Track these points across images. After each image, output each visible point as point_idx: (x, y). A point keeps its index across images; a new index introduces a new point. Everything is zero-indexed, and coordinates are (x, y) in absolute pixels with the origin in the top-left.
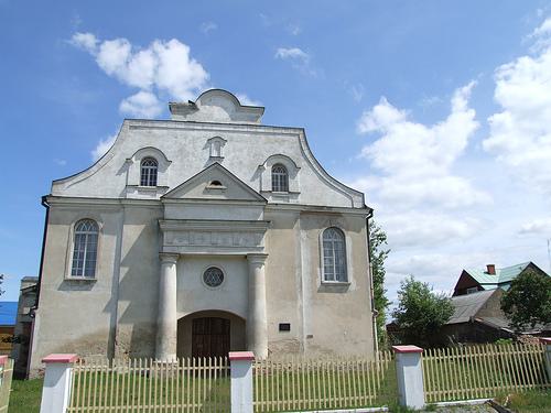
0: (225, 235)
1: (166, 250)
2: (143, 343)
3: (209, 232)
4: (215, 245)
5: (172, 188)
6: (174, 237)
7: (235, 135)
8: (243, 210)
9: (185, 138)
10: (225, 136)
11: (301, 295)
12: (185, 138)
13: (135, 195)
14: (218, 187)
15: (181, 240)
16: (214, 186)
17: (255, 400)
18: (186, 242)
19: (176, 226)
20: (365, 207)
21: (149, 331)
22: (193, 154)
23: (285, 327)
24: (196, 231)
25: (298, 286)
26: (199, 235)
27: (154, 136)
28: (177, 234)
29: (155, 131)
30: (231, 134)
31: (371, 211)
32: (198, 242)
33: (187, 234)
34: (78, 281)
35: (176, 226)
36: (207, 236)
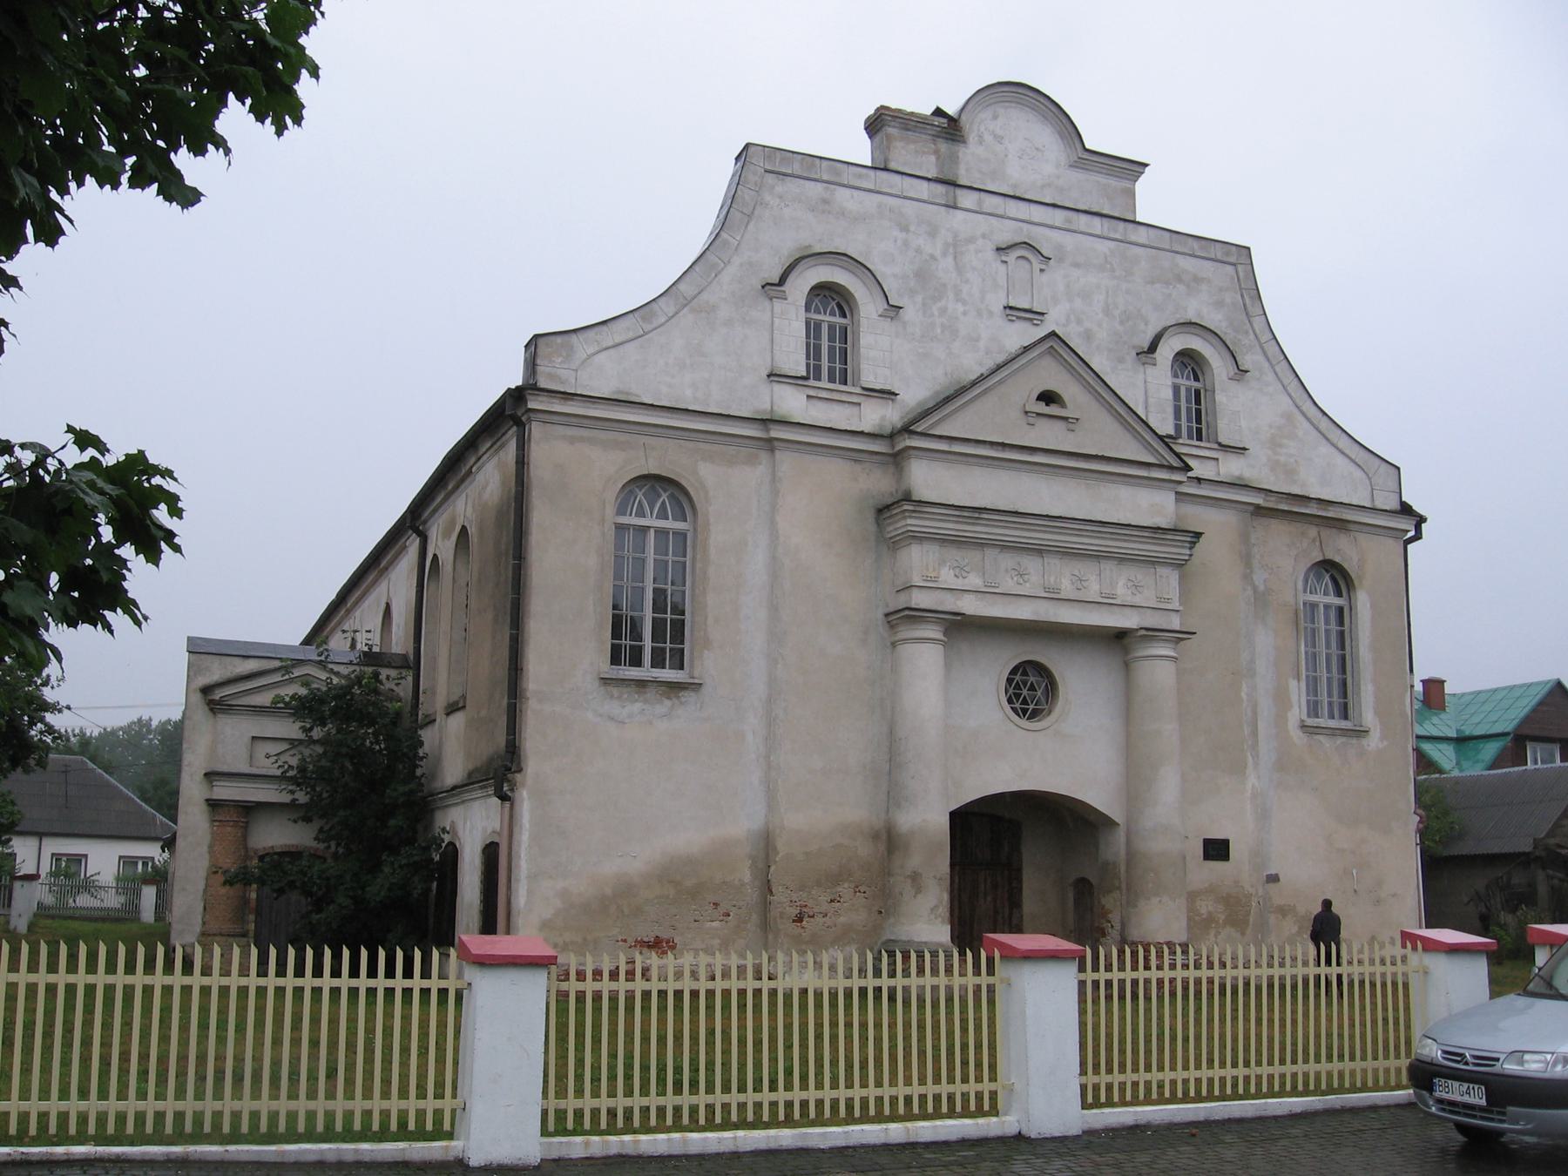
0: (1079, 567)
1: (921, 600)
2: (845, 889)
3: (1039, 551)
4: (1055, 598)
5: (914, 394)
6: (942, 562)
7: (1068, 240)
8: (1124, 493)
9: (933, 233)
10: (1046, 240)
11: (1256, 756)
12: (933, 233)
13: (793, 403)
14: (1053, 410)
15: (960, 571)
16: (1042, 408)
17: (1083, 1072)
18: (974, 581)
19: (950, 527)
20: (1406, 510)
21: (864, 850)
22: (958, 293)
23: (1217, 850)
24: (1005, 547)
25: (1247, 730)
26: (1007, 560)
27: (842, 213)
28: (953, 554)
29: (842, 195)
30: (1055, 235)
31: (1421, 520)
32: (1009, 585)
33: (973, 556)
34: (641, 684)
35: (950, 527)
36: (1031, 564)
